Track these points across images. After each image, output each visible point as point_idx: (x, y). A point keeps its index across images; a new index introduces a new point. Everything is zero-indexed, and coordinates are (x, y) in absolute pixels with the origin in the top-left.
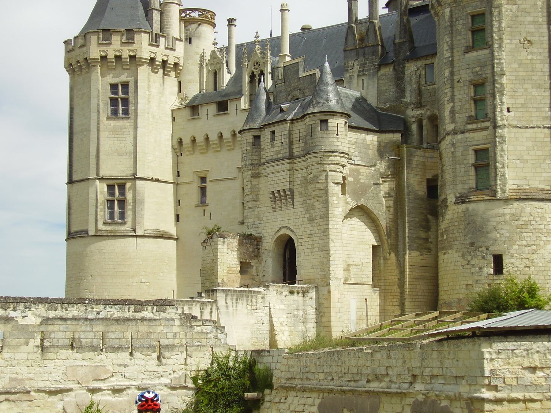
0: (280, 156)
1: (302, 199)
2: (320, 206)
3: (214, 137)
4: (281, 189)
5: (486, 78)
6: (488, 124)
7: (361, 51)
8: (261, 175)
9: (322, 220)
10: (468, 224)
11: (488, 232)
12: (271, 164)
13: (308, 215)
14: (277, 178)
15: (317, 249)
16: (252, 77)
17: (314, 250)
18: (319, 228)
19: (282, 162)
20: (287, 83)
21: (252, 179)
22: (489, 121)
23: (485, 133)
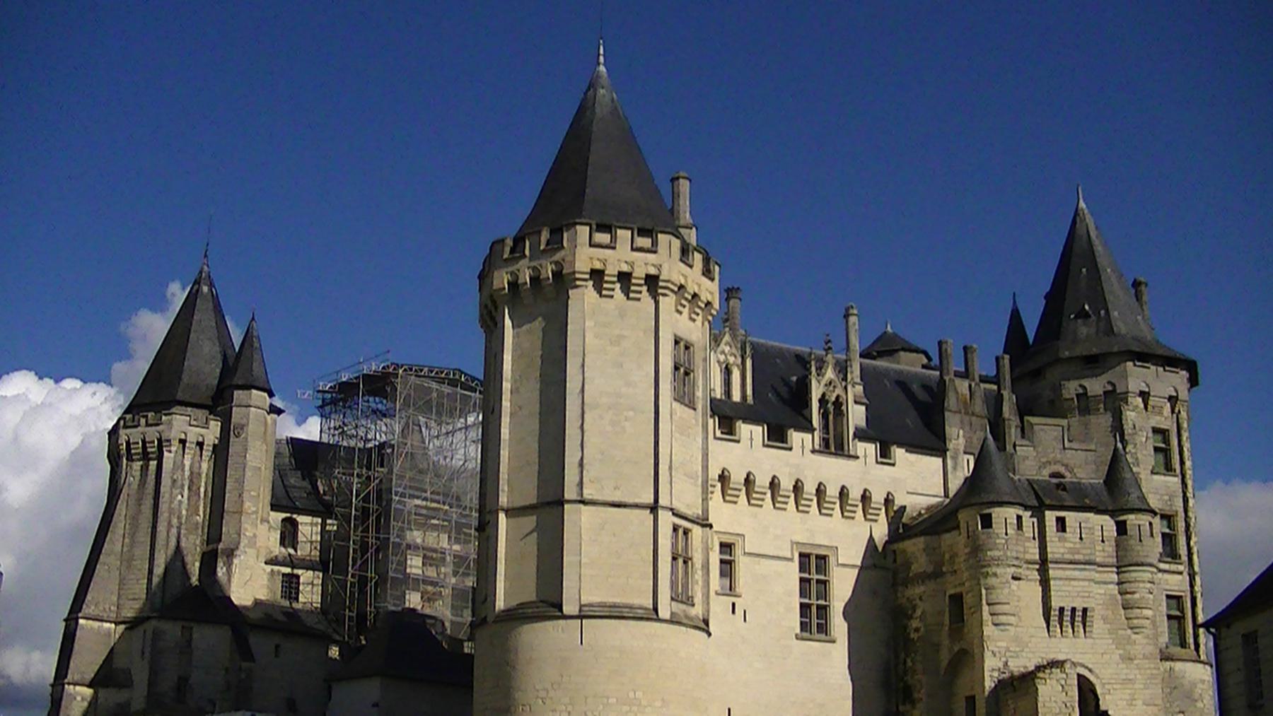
0: (1077, 557)
1: (1108, 626)
2: (1145, 641)
3: (762, 481)
4: (1079, 605)
5: (1177, 512)
6: (1181, 568)
7: (967, 418)
8: (1023, 577)
9: (1147, 661)
10: (1175, 688)
11: (1196, 701)
12: (1060, 566)
13: (1121, 652)
14: (1070, 589)
15: (1140, 702)
16: (823, 401)
17: (1134, 702)
18: (1142, 671)
19: (1082, 566)
20: (1040, 449)
21: (1012, 581)
22: (1181, 564)
23: (1180, 577)
